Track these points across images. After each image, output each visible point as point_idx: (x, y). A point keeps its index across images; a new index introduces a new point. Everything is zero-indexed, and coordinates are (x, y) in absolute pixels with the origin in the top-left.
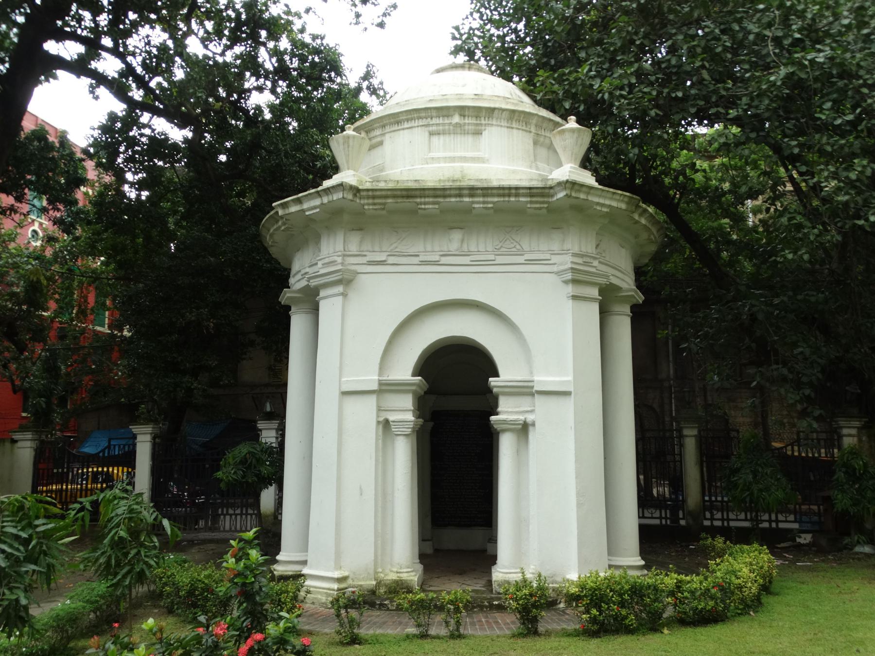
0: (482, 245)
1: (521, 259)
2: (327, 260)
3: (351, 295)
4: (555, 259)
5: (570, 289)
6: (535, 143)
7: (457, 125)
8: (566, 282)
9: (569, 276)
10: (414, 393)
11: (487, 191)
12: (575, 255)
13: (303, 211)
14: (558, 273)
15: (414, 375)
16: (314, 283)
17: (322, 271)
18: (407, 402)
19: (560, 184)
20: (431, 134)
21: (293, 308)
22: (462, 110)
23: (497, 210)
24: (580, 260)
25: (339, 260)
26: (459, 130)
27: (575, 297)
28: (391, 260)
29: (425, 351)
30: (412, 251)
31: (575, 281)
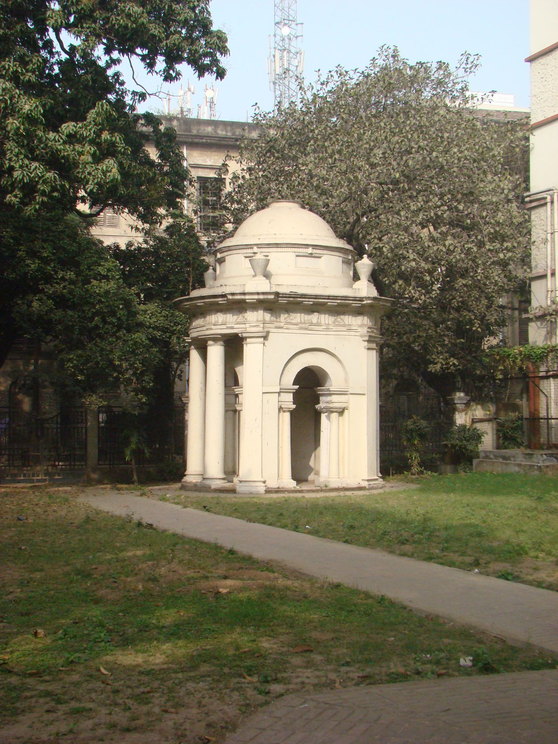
0: (325, 319)
1: (344, 329)
2: (253, 325)
3: (266, 342)
4: (359, 329)
5: (366, 343)
6: (343, 262)
7: (311, 254)
8: (364, 341)
9: (367, 338)
10: (294, 393)
11: (335, 298)
12: (369, 328)
13: (245, 299)
14: (362, 336)
15: (294, 384)
16: (245, 335)
17: (249, 330)
18: (290, 397)
19: (369, 298)
20: (297, 256)
21: (210, 342)
22: (315, 247)
23: (339, 305)
24: (369, 330)
25: (262, 325)
26: (311, 255)
27: (368, 349)
28: (285, 326)
29: (299, 373)
30: (294, 322)
31: (369, 341)
